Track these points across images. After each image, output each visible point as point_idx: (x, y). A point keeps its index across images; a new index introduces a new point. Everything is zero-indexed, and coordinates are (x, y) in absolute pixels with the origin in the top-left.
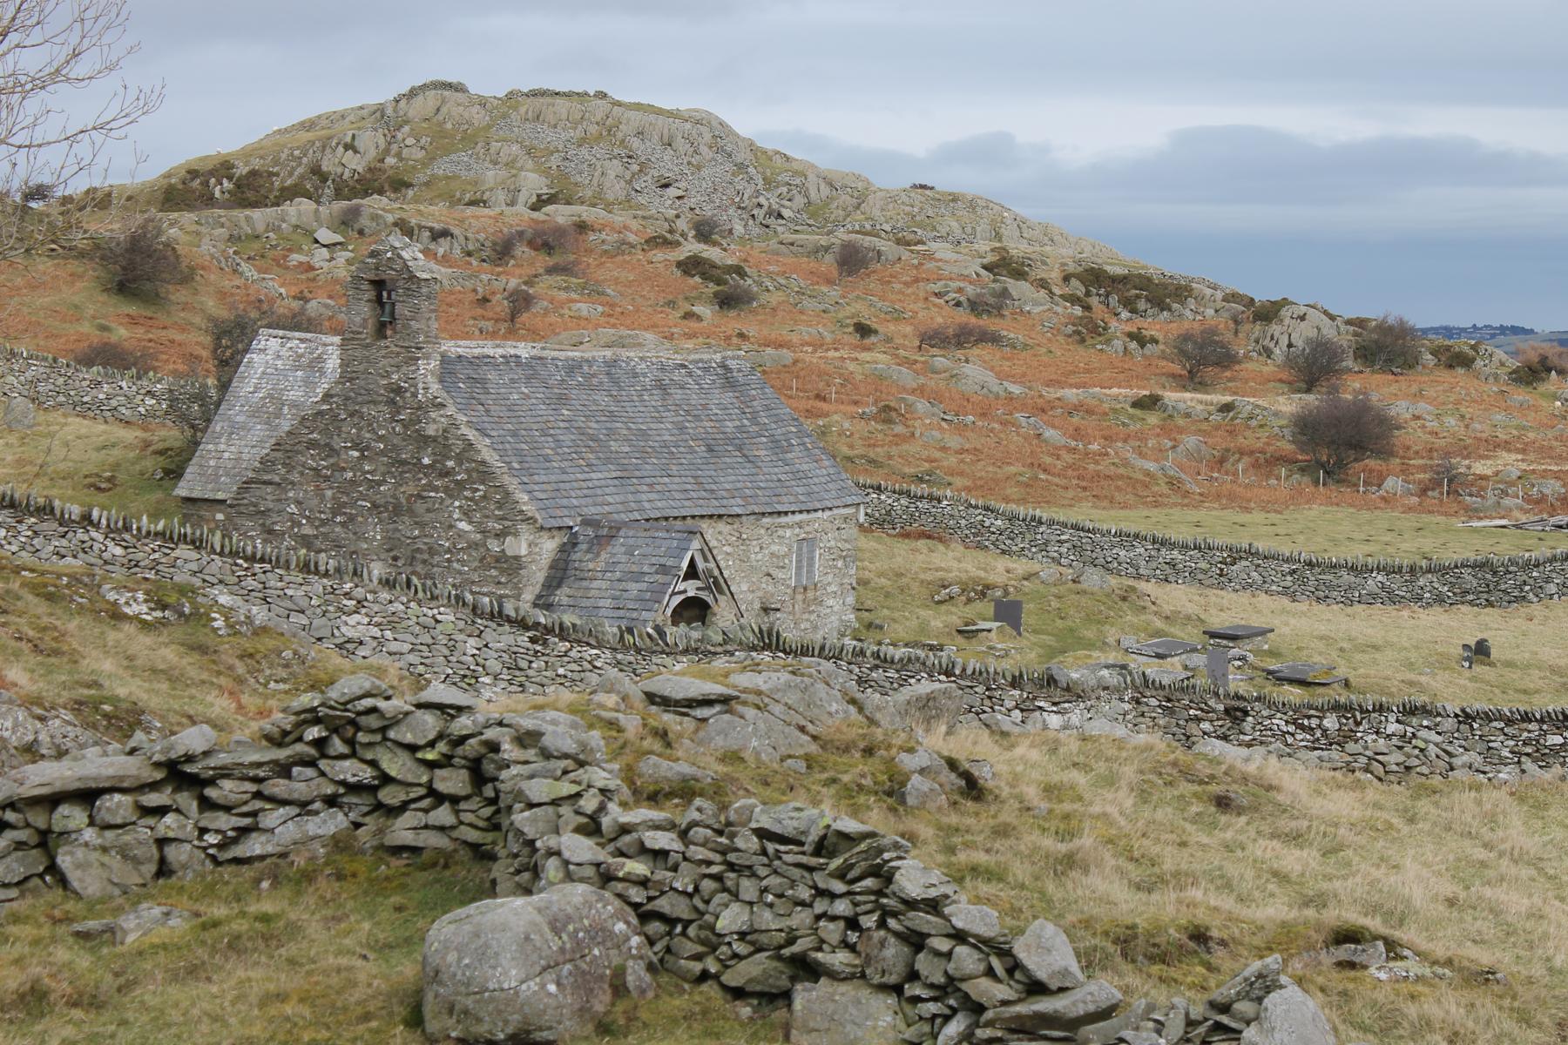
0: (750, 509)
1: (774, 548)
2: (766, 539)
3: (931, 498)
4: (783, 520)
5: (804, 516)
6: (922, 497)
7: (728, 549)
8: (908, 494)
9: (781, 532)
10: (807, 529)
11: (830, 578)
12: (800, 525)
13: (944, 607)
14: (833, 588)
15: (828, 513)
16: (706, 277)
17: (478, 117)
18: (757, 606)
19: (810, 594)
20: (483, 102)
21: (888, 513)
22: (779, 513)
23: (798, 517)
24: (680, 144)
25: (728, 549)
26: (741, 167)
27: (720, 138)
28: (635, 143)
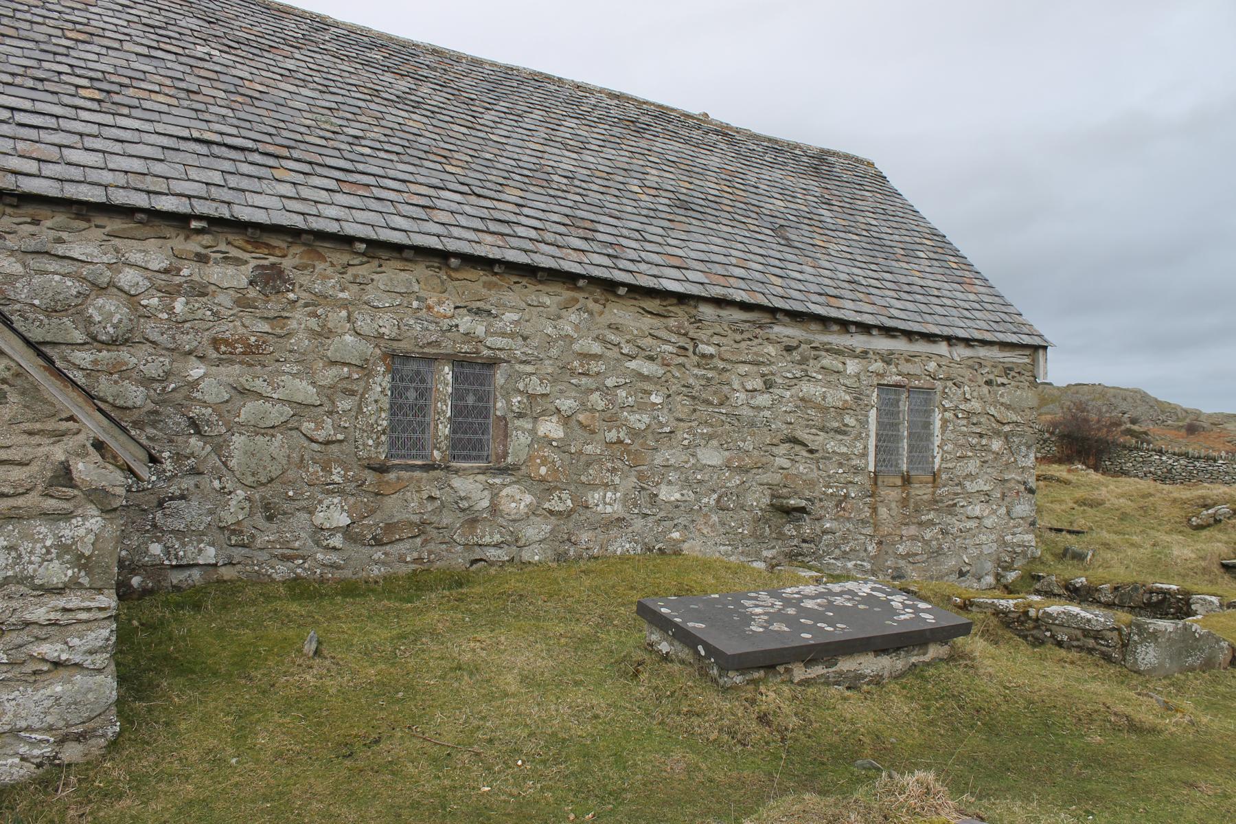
0: (717, 292)
1: (807, 389)
2: (784, 368)
3: (1207, 458)
4: (837, 339)
5: (900, 345)
6: (1199, 458)
7: (647, 368)
8: (1186, 455)
9: (828, 361)
10: (906, 368)
11: (972, 466)
12: (887, 358)
13: (1205, 533)
14: (981, 485)
15: (961, 352)
16: (1132, 436)
17: (1056, 392)
18: (758, 499)
19: (921, 492)
20: (1058, 388)
21: (1169, 471)
22: (824, 321)
23: (882, 344)
24: (1129, 399)
25: (647, 368)
26: (1152, 407)
27: (1144, 397)
28: (1113, 400)
